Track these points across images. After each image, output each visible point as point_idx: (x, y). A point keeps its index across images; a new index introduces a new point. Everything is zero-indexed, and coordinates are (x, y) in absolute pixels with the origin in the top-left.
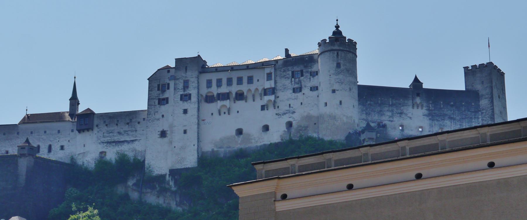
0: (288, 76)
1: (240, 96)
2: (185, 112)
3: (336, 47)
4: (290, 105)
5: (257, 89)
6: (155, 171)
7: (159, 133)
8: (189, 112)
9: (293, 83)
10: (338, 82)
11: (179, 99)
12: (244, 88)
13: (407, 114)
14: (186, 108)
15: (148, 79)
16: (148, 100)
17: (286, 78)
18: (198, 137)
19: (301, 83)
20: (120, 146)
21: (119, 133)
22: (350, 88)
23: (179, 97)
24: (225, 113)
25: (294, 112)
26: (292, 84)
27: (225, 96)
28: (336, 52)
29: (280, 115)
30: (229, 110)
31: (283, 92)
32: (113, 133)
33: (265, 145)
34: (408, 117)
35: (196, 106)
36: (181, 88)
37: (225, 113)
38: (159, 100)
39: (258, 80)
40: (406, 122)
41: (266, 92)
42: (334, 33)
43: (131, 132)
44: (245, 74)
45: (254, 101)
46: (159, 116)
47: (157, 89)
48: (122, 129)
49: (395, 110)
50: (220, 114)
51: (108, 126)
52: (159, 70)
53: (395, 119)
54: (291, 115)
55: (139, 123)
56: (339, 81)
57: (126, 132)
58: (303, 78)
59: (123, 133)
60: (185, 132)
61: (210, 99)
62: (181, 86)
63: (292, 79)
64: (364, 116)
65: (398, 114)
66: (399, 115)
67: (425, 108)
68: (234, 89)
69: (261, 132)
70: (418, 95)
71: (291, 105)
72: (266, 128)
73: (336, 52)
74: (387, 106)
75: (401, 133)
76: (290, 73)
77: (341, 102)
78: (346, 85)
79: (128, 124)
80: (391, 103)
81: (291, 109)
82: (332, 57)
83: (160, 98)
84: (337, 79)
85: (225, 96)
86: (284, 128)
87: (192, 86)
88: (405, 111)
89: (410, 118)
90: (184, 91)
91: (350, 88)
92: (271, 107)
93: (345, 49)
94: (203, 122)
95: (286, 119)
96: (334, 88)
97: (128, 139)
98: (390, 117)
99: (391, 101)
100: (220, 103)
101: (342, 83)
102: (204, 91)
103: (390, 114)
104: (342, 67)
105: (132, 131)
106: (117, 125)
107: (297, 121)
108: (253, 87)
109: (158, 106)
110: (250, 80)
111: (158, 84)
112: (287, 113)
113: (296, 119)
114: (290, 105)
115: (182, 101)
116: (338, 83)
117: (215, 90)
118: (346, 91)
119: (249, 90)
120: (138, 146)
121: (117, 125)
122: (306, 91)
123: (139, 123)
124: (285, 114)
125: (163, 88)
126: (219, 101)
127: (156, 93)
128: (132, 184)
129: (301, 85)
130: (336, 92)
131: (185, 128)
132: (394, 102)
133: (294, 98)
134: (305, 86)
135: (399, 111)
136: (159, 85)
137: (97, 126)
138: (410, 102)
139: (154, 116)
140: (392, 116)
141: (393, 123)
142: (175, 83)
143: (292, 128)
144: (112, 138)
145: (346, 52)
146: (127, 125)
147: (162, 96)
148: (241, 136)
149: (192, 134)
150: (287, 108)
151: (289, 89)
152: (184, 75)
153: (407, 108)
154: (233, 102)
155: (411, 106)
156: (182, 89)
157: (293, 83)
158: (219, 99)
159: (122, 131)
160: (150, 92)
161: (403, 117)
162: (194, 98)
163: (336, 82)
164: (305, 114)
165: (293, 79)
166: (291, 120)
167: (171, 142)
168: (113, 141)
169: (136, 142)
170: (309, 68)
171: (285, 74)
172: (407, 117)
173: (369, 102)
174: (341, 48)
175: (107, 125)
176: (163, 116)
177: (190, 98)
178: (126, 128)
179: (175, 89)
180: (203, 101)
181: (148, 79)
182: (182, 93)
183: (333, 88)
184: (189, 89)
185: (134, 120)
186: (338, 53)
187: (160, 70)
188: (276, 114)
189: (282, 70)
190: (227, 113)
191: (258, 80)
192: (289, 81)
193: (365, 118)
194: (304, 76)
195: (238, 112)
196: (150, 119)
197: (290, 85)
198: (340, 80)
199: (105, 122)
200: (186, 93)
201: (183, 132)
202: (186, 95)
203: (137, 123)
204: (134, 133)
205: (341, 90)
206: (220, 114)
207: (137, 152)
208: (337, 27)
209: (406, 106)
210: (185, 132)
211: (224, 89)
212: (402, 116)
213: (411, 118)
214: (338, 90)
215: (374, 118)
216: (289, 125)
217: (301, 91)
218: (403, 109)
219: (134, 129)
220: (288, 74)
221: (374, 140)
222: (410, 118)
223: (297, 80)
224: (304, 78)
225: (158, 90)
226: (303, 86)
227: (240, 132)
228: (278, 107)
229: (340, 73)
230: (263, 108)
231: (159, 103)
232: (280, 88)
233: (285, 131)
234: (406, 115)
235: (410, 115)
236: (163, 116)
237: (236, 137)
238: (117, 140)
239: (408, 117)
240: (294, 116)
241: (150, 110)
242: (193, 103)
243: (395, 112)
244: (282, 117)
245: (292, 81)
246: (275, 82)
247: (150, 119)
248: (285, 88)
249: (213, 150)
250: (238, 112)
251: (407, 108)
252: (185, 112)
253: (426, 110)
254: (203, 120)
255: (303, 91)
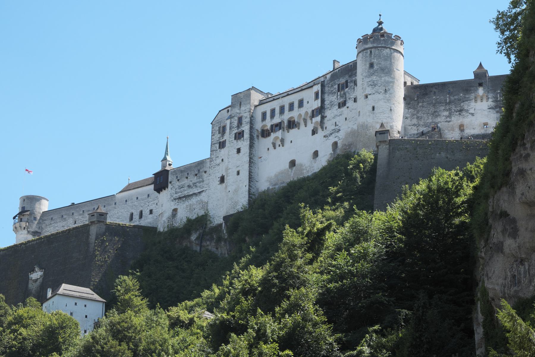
0: (334, 91)
1: (292, 124)
2: (239, 151)
3: (370, 45)
4: (336, 123)
5: (307, 113)
6: (215, 221)
7: (219, 179)
8: (242, 151)
9: (339, 97)
10: (371, 85)
11: (234, 138)
12: (295, 114)
13: (468, 111)
14: (239, 147)
15: (212, 124)
16: (211, 145)
17: (332, 94)
18: (249, 176)
19: (345, 95)
20: (189, 200)
21: (189, 186)
22: (386, 89)
23: (234, 136)
24: (279, 146)
25: (339, 130)
26: (338, 100)
27: (278, 126)
28: (369, 51)
29: (327, 136)
30: (282, 141)
31: (330, 109)
32: (183, 187)
33: (315, 173)
34: (470, 113)
35: (248, 143)
36: (235, 127)
37: (279, 146)
38: (220, 143)
39: (308, 102)
40: (467, 120)
41: (314, 114)
42: (375, 30)
43: (199, 183)
44: (295, 99)
45: (306, 126)
46: (219, 161)
47: (218, 132)
48: (191, 181)
49: (453, 108)
50: (275, 148)
51: (180, 180)
52: (220, 111)
53: (453, 118)
54: (337, 134)
55: (205, 172)
56: (372, 84)
57: (195, 185)
58: (347, 89)
59: (192, 186)
60: (238, 173)
61: (265, 133)
62: (235, 123)
63: (338, 93)
64: (415, 121)
65: (456, 112)
66: (458, 113)
67: (490, 100)
68: (287, 116)
69: (312, 160)
70: (480, 85)
71: (337, 124)
72: (316, 154)
73: (369, 51)
74: (444, 104)
75: (461, 134)
76: (336, 86)
77: (373, 108)
78: (380, 87)
79: (196, 175)
80: (448, 101)
81: (337, 127)
82: (364, 58)
83: (221, 141)
84: (370, 81)
85: (278, 126)
86: (330, 151)
87: (245, 121)
88: (466, 107)
89: (473, 114)
90: (238, 129)
91: (386, 89)
92: (320, 130)
93: (380, 45)
94: (260, 159)
95: (332, 139)
96: (367, 93)
97: (196, 192)
98: (447, 117)
99: (448, 99)
100: (273, 135)
101: (375, 85)
102: (259, 126)
103: (446, 113)
104: (376, 67)
105: (200, 182)
106: (187, 178)
107: (342, 140)
108: (303, 111)
109: (219, 150)
110: (301, 103)
111: (219, 126)
112: (333, 133)
113: (340, 137)
114: (336, 123)
115: (236, 141)
116: (370, 86)
117: (269, 123)
118: (379, 93)
119: (300, 115)
120: (203, 197)
121: (187, 178)
122: (350, 103)
123: (205, 172)
124: (331, 134)
125: (223, 130)
126: (272, 133)
127: (217, 136)
128: (195, 238)
129: (346, 98)
130: (369, 96)
131: (238, 169)
132: (452, 98)
133: (339, 114)
134: (349, 98)
135: (459, 109)
136: (220, 127)
137: (171, 182)
138: (472, 96)
139: (215, 162)
140: (450, 116)
141: (451, 123)
142: (230, 122)
143: (337, 149)
144: (183, 193)
145: (380, 49)
146: (196, 177)
147: (223, 138)
148: (294, 168)
149: (245, 174)
150: (333, 127)
151: (335, 105)
152: (238, 111)
153: (469, 103)
154: (286, 131)
155: (474, 100)
156: (236, 127)
157: (339, 97)
158: (272, 132)
159: (191, 184)
160: (213, 137)
161: (463, 115)
162: (247, 135)
163: (368, 85)
164: (349, 130)
165: (339, 93)
166: (336, 139)
167: (226, 187)
168: (183, 195)
169: (203, 193)
170: (353, 77)
171: (332, 89)
172: (468, 114)
173: (420, 104)
174: (375, 45)
175: (178, 180)
176: (222, 160)
177: (243, 136)
178: (195, 180)
179: (230, 129)
180: (260, 136)
181: (212, 124)
182: (236, 131)
183: (365, 94)
184: (243, 125)
185: (201, 170)
186: (371, 52)
187: (222, 112)
188: (324, 136)
189: (330, 86)
190: (281, 145)
191: (308, 102)
192: (335, 97)
193: (416, 123)
194: (349, 87)
195: (291, 142)
196: (212, 166)
197: (336, 100)
198: (373, 82)
199: (177, 177)
200: (240, 130)
201: (236, 173)
202: (239, 133)
203: (204, 173)
204: (202, 183)
205: (374, 94)
206: (275, 148)
207: (204, 204)
208: (380, 23)
209: (467, 101)
210: (238, 173)
211: (277, 120)
212: (462, 114)
213: (473, 114)
214: (370, 95)
215: (428, 121)
216: (335, 144)
217: (345, 105)
218: (463, 105)
219: (201, 180)
220: (335, 88)
221: (387, 143)
222: (473, 114)
223: (342, 92)
224: (348, 90)
225: (219, 133)
226: (347, 99)
227: (293, 163)
228: (326, 127)
229: (373, 74)
230: (314, 132)
231: (220, 148)
232: (328, 106)
233: (331, 154)
234: (467, 111)
235: (472, 111)
236: (222, 160)
237: (290, 170)
238: (187, 194)
239: (470, 113)
240: (339, 134)
241: (213, 156)
242: (246, 140)
243: (453, 111)
244: (330, 138)
245: (338, 96)
246: (323, 101)
247: (212, 166)
248: (332, 105)
249: (268, 188)
250: (291, 142)
251: (469, 103)
252: (239, 151)
253: (492, 101)
254: (260, 158)
255: (347, 105)
